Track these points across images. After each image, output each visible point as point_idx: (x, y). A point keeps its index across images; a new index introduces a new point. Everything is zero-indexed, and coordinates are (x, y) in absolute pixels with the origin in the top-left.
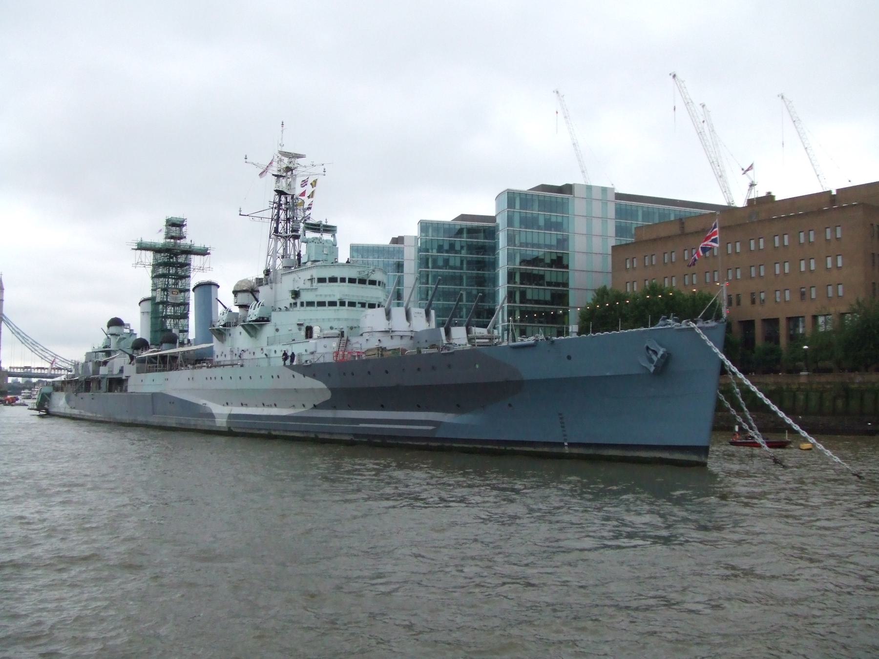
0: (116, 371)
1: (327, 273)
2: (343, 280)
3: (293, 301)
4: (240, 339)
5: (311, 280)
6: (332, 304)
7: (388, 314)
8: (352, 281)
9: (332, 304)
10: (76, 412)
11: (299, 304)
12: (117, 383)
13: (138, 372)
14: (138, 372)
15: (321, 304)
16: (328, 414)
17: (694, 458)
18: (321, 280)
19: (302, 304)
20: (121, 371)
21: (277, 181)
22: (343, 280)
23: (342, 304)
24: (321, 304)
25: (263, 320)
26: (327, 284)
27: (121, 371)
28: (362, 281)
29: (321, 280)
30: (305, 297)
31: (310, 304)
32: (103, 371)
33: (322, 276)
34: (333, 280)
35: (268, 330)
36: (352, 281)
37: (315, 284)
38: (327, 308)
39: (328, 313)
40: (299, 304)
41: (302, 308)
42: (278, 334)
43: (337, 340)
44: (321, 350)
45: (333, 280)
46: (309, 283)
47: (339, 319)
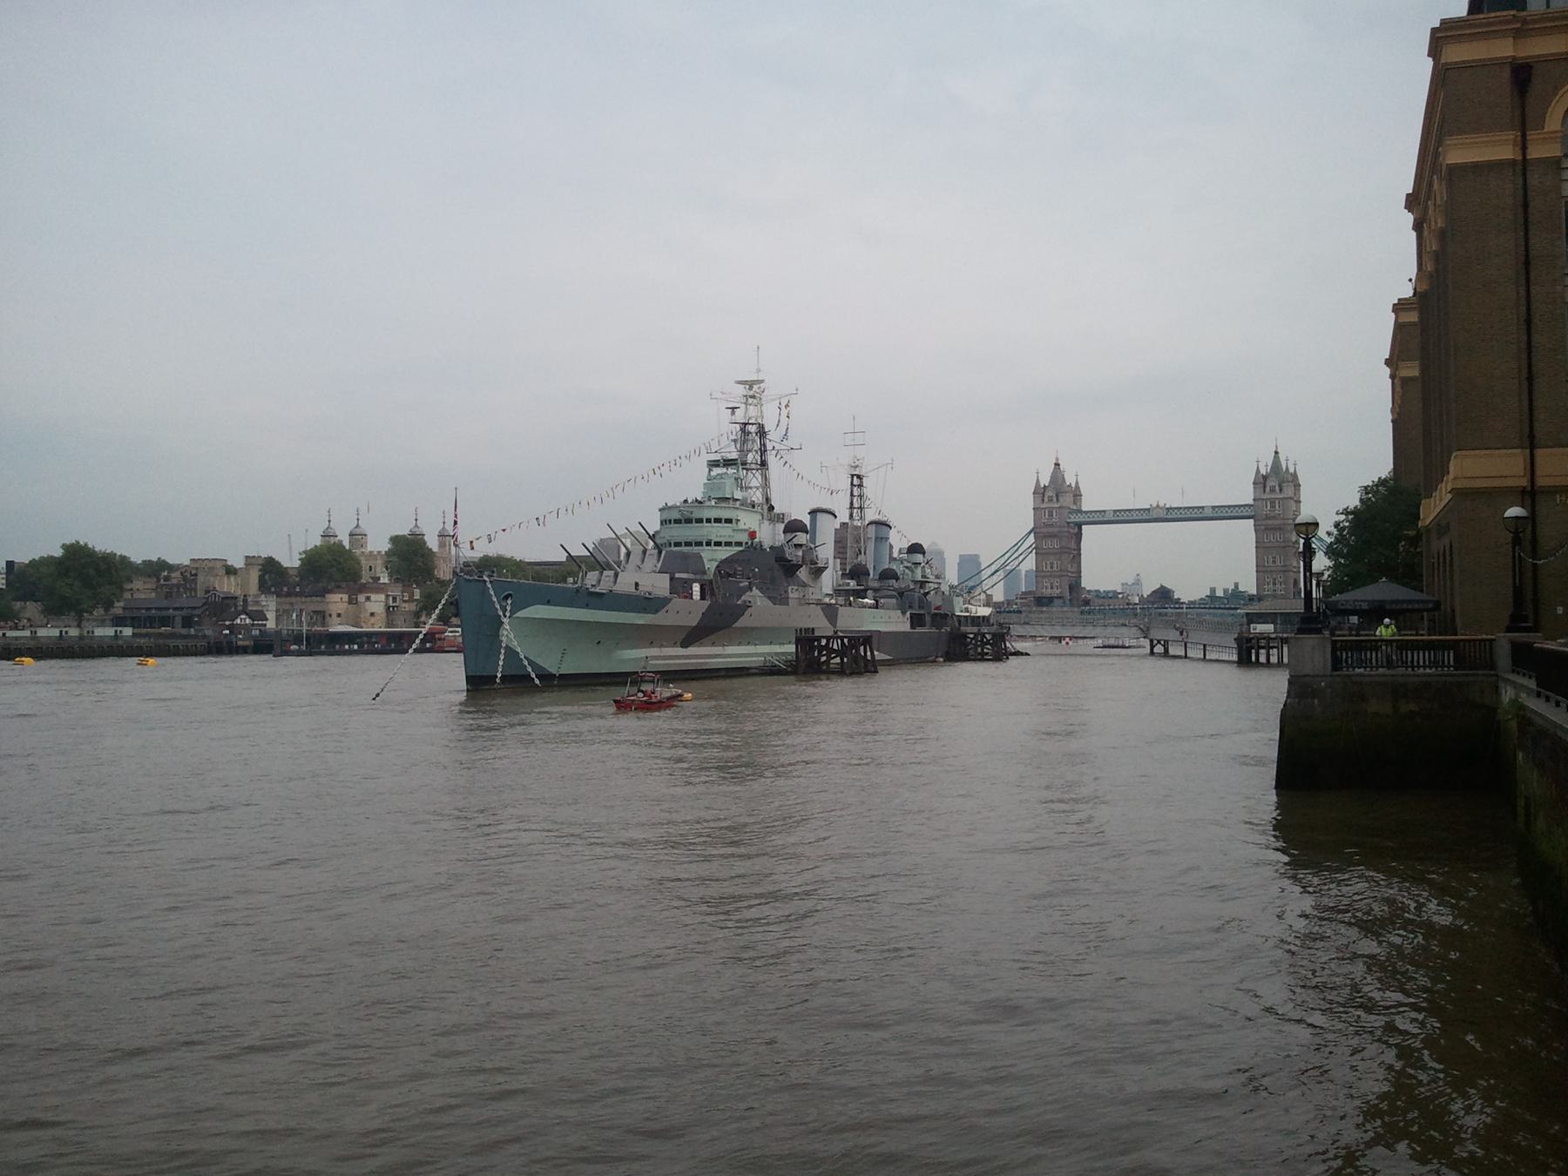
8: (677, 521)
28: (689, 521)
36: (677, 521)
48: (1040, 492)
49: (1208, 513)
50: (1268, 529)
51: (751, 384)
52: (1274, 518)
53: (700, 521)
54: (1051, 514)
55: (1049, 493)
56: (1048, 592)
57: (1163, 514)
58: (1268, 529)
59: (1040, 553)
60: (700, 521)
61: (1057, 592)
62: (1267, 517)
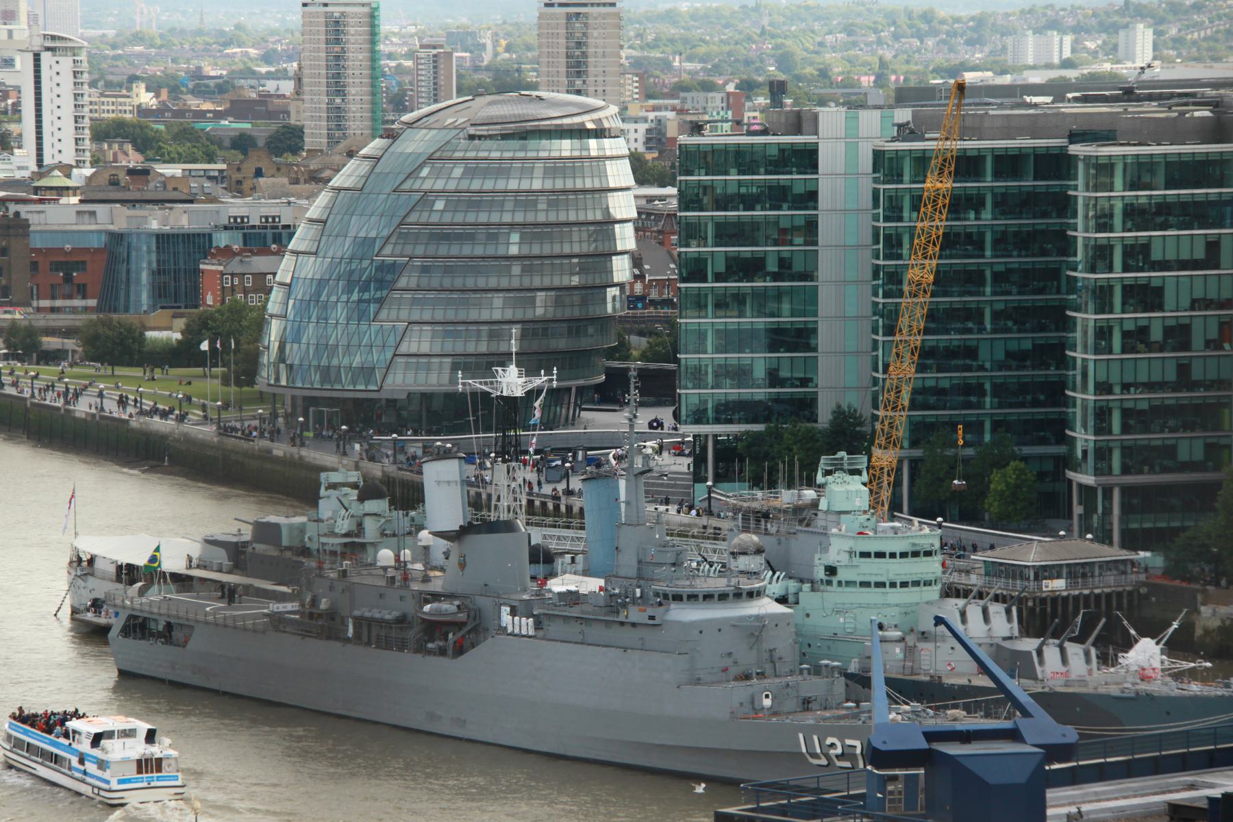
1: (873, 547)
2: (893, 555)
3: (824, 578)
5: (851, 553)
6: (880, 585)
8: (904, 555)
9: (880, 585)
11: (835, 583)
19: (840, 583)
22: (893, 555)
23: (893, 585)
26: (873, 559)
28: (916, 554)
30: (842, 575)
33: (866, 550)
34: (880, 555)
36: (904, 555)
37: (857, 560)
38: (873, 590)
40: (835, 583)
41: (840, 589)
45: (880, 555)
46: (847, 555)
47: (889, 605)
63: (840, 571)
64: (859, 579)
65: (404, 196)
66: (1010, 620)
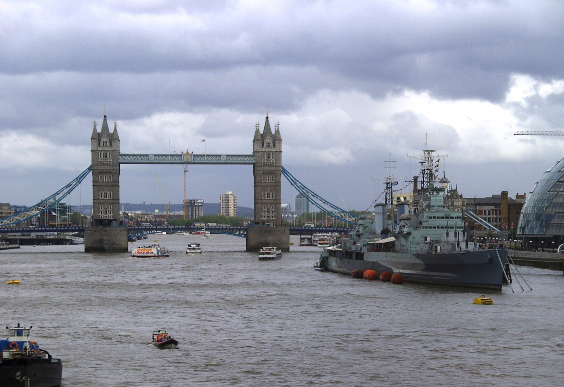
0: (359, 249)
2: (438, 218)
4: (403, 240)
6: (434, 227)
7: (447, 234)
8: (442, 218)
9: (434, 227)
10: (341, 269)
12: (360, 256)
13: (368, 251)
14: (368, 251)
15: (430, 227)
16: (425, 273)
17: (497, 287)
18: (430, 218)
20: (361, 249)
21: (422, 165)
22: (438, 218)
23: (438, 227)
24: (430, 227)
25: (409, 233)
27: (361, 249)
28: (447, 218)
29: (430, 218)
30: (424, 224)
31: (426, 227)
32: (354, 248)
33: (430, 216)
34: (435, 217)
35: (411, 238)
36: (442, 218)
39: (432, 231)
42: (414, 240)
43: (429, 245)
44: (424, 249)
45: (435, 217)
48: (97, 138)
49: (224, 159)
50: (265, 173)
51: (429, 152)
52: (271, 165)
53: (452, 218)
54: (105, 156)
55: (105, 139)
56: (103, 216)
57: (190, 159)
58: (265, 173)
59: (96, 184)
60: (452, 218)
61: (110, 216)
62: (265, 165)
63: (423, 223)
64: (428, 226)
65: (561, 173)
66: (464, 237)
